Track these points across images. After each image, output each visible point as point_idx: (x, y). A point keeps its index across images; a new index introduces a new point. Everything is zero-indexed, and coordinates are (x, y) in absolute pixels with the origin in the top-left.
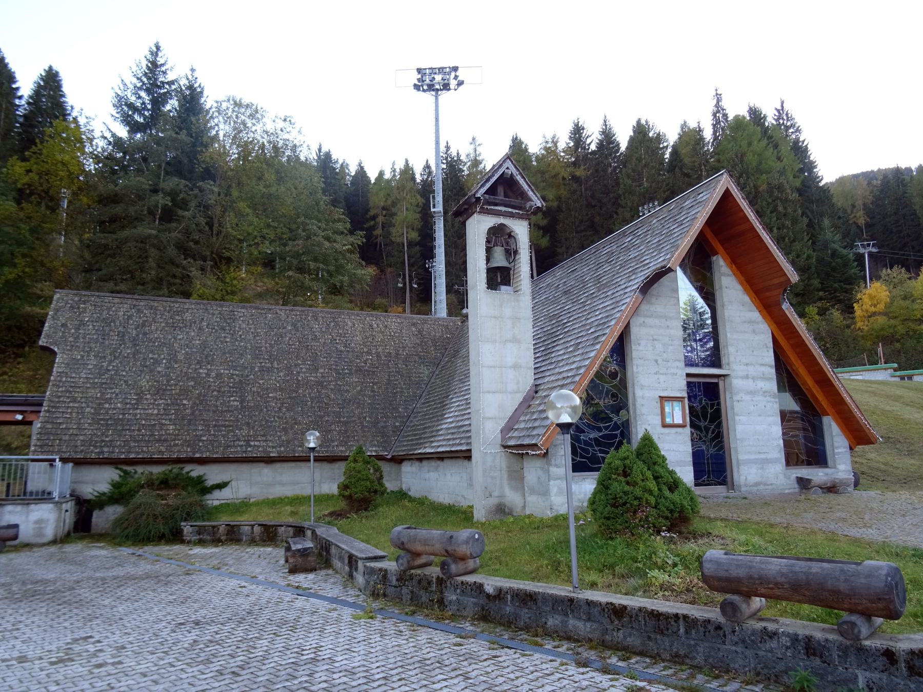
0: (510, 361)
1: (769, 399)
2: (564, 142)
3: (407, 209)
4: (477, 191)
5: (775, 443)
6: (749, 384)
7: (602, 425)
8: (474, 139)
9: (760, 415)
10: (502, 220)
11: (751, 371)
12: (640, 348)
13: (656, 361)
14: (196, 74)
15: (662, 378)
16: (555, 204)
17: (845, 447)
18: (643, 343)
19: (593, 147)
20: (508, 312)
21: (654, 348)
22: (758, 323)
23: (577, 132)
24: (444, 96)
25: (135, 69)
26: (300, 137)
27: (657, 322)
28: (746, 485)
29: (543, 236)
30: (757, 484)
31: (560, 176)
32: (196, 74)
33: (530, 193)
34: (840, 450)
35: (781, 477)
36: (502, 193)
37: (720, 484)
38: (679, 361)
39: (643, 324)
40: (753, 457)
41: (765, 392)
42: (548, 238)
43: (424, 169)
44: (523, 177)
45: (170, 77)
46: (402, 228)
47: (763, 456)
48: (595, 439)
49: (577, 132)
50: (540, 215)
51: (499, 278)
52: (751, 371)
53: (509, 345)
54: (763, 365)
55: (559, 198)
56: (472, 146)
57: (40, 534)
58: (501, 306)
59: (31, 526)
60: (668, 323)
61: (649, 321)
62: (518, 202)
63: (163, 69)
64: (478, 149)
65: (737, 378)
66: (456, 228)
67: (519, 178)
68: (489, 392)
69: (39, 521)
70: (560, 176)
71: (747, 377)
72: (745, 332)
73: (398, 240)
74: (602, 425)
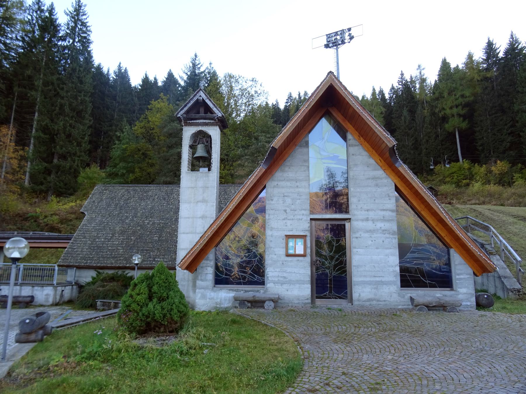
0: (199, 214)
1: (388, 235)
2: (479, 55)
4: (178, 114)
5: (391, 269)
6: (370, 225)
8: (419, 66)
9: (377, 248)
10: (200, 128)
11: (371, 215)
12: (273, 202)
13: (285, 211)
14: (212, 66)
15: (289, 223)
16: (472, 98)
17: (469, 274)
18: (275, 199)
19: (501, 55)
20: (200, 183)
21: (284, 202)
22: (381, 179)
23: (490, 48)
24: (342, 48)
25: (184, 69)
26: (262, 88)
27: (288, 184)
28: (359, 300)
29: (463, 121)
30: (369, 300)
31: (475, 79)
32: (212, 66)
33: (215, 109)
34: (462, 277)
35: (395, 296)
36: (203, 112)
37: (340, 298)
38: (305, 210)
39: (277, 186)
40: (368, 279)
41: (383, 231)
42: (467, 122)
43: (391, 90)
44: (210, 100)
45: (202, 69)
47: (377, 279)
49: (490, 48)
50: (460, 107)
51: (201, 162)
52: (371, 215)
53: (199, 204)
54: (384, 210)
55: (475, 95)
56: (419, 71)
57: (47, 300)
58: (196, 180)
59: (44, 297)
60: (298, 184)
61: (281, 183)
62: (209, 115)
63: (199, 66)
64: (423, 72)
65: (357, 220)
66: (407, 124)
67: (208, 101)
68: (184, 233)
69: (47, 295)
70: (475, 79)
71: (367, 220)
72: (368, 186)
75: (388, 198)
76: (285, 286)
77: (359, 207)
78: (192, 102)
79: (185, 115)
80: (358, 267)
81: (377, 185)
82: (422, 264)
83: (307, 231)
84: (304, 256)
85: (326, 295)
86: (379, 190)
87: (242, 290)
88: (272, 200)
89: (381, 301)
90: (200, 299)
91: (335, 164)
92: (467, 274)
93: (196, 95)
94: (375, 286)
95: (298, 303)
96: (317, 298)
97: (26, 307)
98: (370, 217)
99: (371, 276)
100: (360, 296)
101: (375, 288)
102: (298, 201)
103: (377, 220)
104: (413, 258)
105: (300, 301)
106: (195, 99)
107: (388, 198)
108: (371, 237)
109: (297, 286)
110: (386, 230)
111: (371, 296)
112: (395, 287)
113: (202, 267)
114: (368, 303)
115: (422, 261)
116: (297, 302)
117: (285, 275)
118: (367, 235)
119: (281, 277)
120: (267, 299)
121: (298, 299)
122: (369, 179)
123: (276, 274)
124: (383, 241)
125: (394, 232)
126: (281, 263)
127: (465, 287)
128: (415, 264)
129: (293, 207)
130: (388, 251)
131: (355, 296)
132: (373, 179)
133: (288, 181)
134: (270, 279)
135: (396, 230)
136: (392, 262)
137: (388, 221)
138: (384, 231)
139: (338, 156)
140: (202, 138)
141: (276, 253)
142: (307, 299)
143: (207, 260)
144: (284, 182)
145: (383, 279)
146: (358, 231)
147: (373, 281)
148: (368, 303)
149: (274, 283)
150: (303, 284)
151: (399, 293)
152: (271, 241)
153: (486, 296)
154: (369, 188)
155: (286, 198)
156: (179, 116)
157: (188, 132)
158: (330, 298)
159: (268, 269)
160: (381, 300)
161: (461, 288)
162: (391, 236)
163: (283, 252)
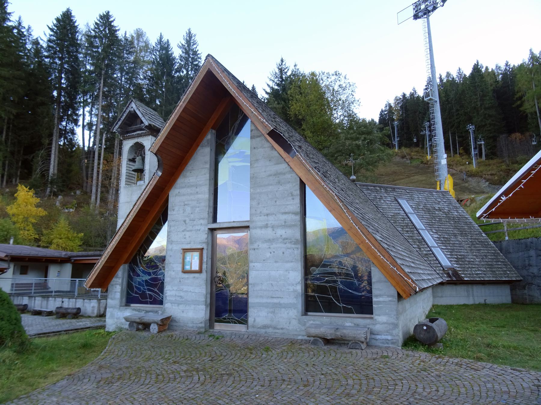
1: (289, 245)
3: (536, 86)
5: (291, 288)
6: (269, 233)
7: (151, 271)
9: (276, 262)
11: (271, 220)
12: (174, 213)
13: (185, 221)
14: (297, 68)
15: (188, 234)
17: (392, 296)
18: (176, 208)
21: (184, 211)
22: (284, 174)
24: (433, 16)
25: (270, 76)
26: (347, 81)
27: (189, 190)
28: (253, 327)
30: (265, 327)
32: (297, 68)
34: (381, 299)
35: (295, 322)
37: (240, 323)
38: (203, 219)
39: (179, 194)
40: (264, 300)
41: (284, 239)
45: (289, 73)
46: (533, 100)
47: (276, 301)
48: (146, 281)
52: (271, 220)
54: (285, 213)
58: (132, 194)
59: (91, 309)
60: (198, 190)
61: (183, 191)
63: (285, 71)
65: (255, 228)
69: (93, 307)
71: (266, 226)
72: (269, 185)
73: (532, 110)
74: (151, 271)
75: (291, 198)
76: (182, 307)
77: (258, 212)
78: (125, 115)
79: (119, 130)
80: (254, 285)
81: (279, 183)
82: (335, 282)
83: (204, 243)
84: (200, 271)
85: (225, 319)
86: (281, 188)
87: (144, 310)
88: (173, 210)
89: (278, 329)
90: (109, 318)
91: (241, 161)
92: (388, 296)
93: (128, 106)
94: (272, 310)
95: (192, 327)
96: (217, 321)
97: (73, 318)
98: (269, 223)
99: (268, 297)
100: (255, 321)
101: (272, 312)
102: (197, 209)
103: (278, 226)
104: (325, 273)
105: (195, 325)
106: (128, 111)
107: (291, 198)
108: (270, 248)
109: (193, 307)
110: (287, 239)
111: (267, 322)
112: (295, 311)
113: (112, 285)
114: (263, 331)
115: (335, 278)
116: (191, 325)
117: (182, 294)
118: (265, 245)
119: (178, 296)
120: (152, 321)
121: (193, 323)
122: (271, 175)
123: (173, 293)
124: (283, 253)
125: (297, 240)
126: (178, 280)
127: (385, 314)
128: (327, 282)
129: (192, 216)
130: (289, 265)
131: (250, 320)
132: (275, 175)
133: (188, 187)
134: (168, 298)
135: (299, 238)
136: (293, 277)
137: (290, 226)
138: (285, 240)
139: (244, 152)
140: (139, 149)
141: (175, 269)
142: (201, 323)
143: (117, 277)
144: (185, 189)
145: (282, 301)
146: (256, 242)
147: (270, 303)
148: (263, 331)
149: (171, 303)
150: (198, 305)
151: (299, 320)
152: (171, 256)
153: (425, 328)
154: (270, 187)
155: (186, 206)
156: (114, 131)
157: (128, 145)
158: (229, 322)
159: (167, 287)
160: (278, 327)
161: (379, 315)
162: (293, 246)
163: (180, 269)
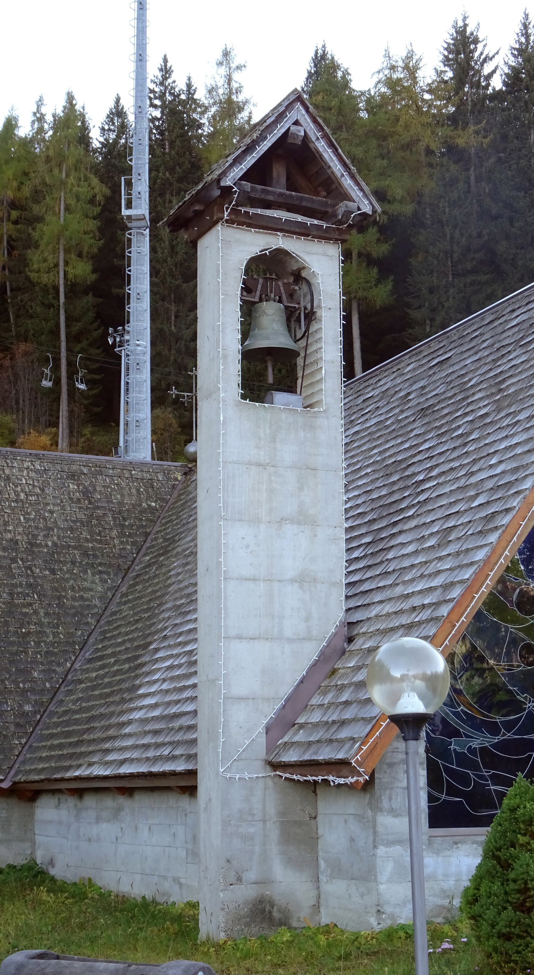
0: (290, 566)
2: (431, 67)
3: (67, 209)
4: (224, 174)
7: (498, 719)
8: (226, 54)
10: (280, 242)
16: (408, 209)
19: (497, 83)
20: (288, 453)
23: (462, 48)
29: (378, 282)
31: (422, 146)
33: (347, 182)
36: (283, 180)
42: (390, 286)
43: (110, 118)
44: (331, 145)
46: (55, 251)
48: (483, 750)
49: (462, 48)
50: (373, 233)
51: (269, 373)
53: (289, 529)
55: (417, 196)
56: (223, 70)
58: (273, 439)
62: (318, 200)
64: (236, 76)
66: (179, 257)
67: (321, 146)
68: (239, 638)
70: (422, 146)
73: (45, 279)
74: (498, 719)
90: (390, 881)
